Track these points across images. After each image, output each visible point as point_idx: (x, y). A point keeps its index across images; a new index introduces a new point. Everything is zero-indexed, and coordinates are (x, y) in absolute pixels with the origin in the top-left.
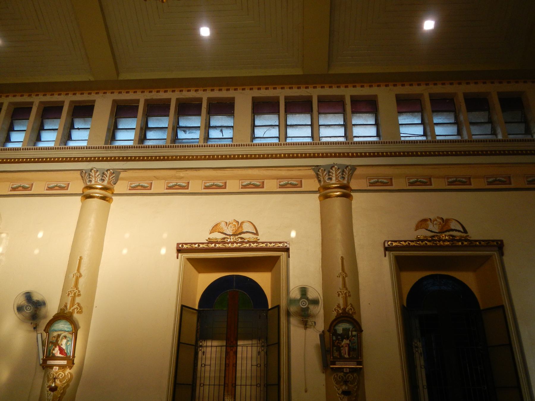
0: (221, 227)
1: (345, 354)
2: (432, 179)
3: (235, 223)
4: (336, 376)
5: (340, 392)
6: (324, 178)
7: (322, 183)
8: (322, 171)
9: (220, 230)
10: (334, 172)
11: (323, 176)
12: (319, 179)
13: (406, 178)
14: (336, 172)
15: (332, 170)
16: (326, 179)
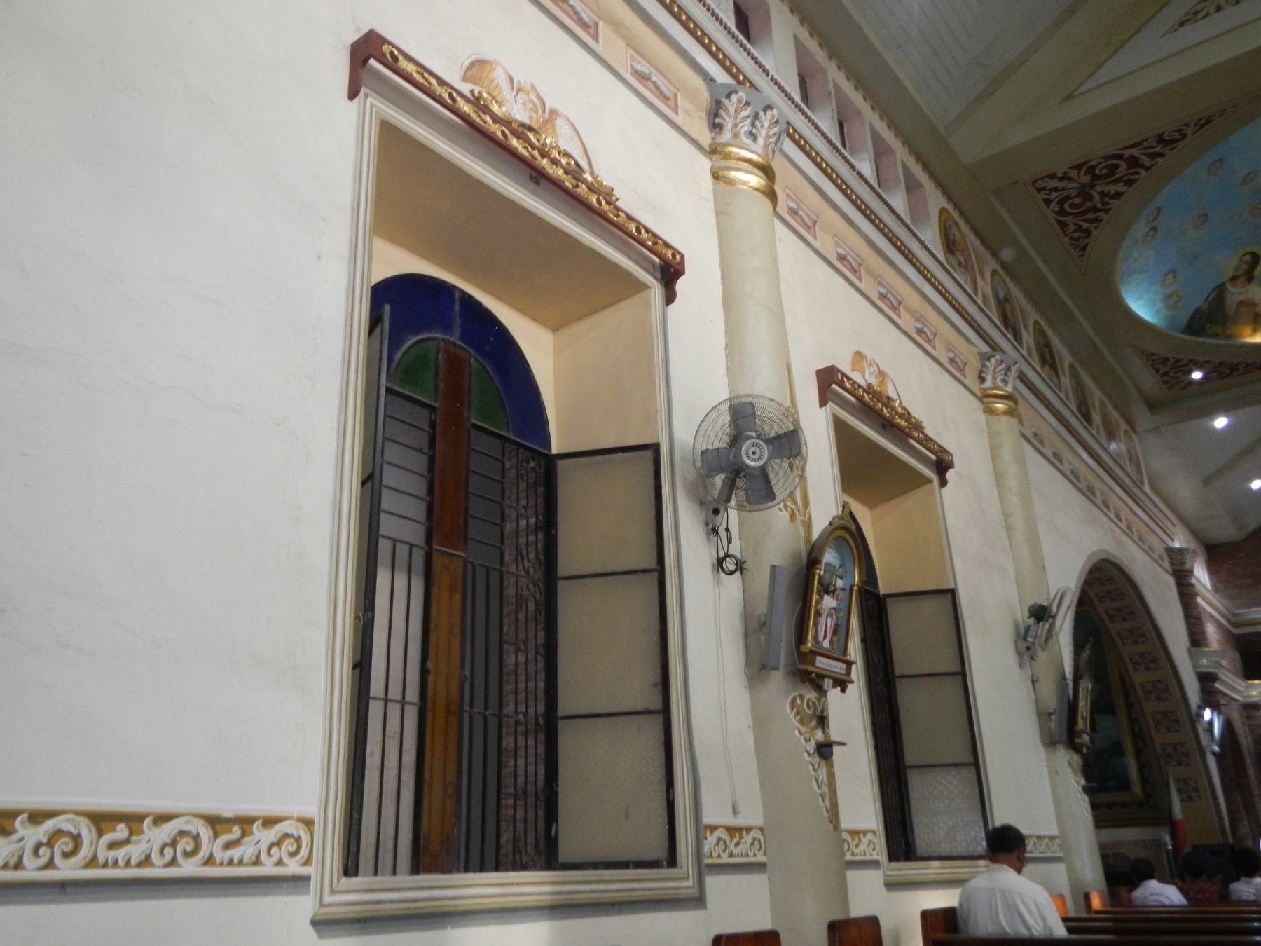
0: (496, 82)
1: (825, 637)
2: (862, 268)
3: (532, 96)
4: (798, 701)
5: (811, 747)
6: (736, 126)
7: (726, 136)
8: (740, 101)
9: (492, 87)
10: (766, 124)
11: (736, 118)
12: (717, 120)
13: (832, 239)
14: (769, 128)
15: (765, 114)
16: (742, 131)
